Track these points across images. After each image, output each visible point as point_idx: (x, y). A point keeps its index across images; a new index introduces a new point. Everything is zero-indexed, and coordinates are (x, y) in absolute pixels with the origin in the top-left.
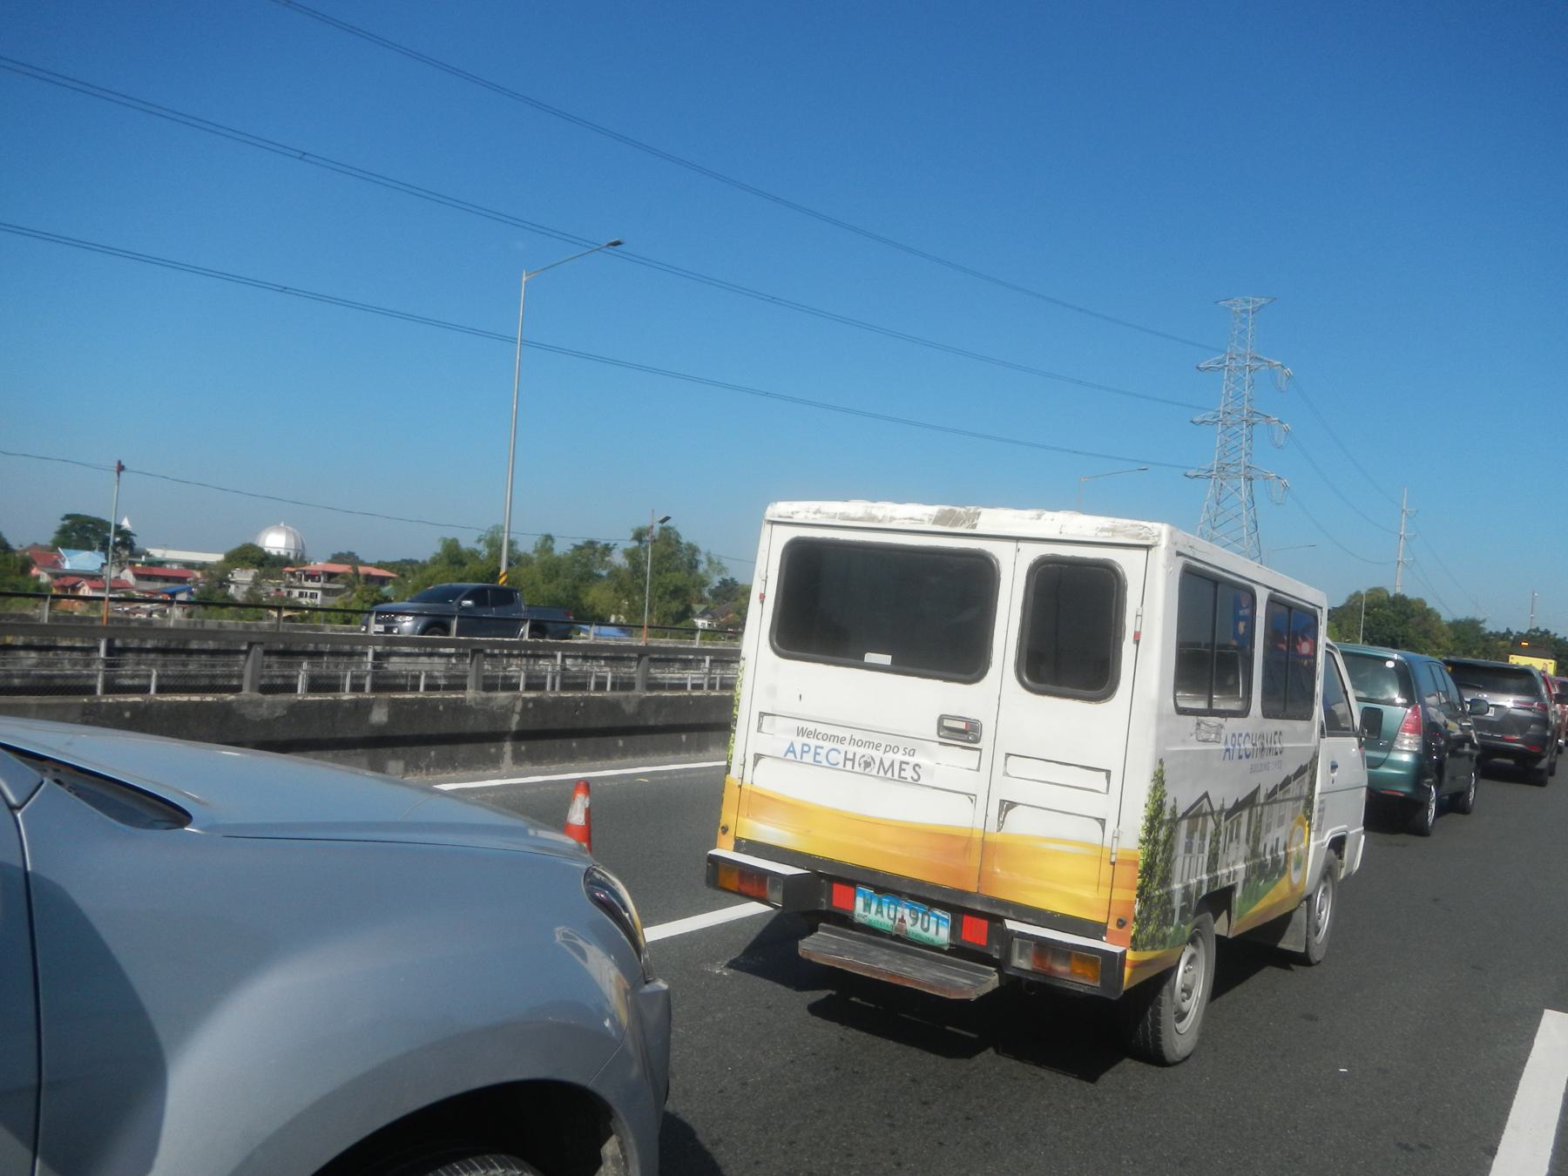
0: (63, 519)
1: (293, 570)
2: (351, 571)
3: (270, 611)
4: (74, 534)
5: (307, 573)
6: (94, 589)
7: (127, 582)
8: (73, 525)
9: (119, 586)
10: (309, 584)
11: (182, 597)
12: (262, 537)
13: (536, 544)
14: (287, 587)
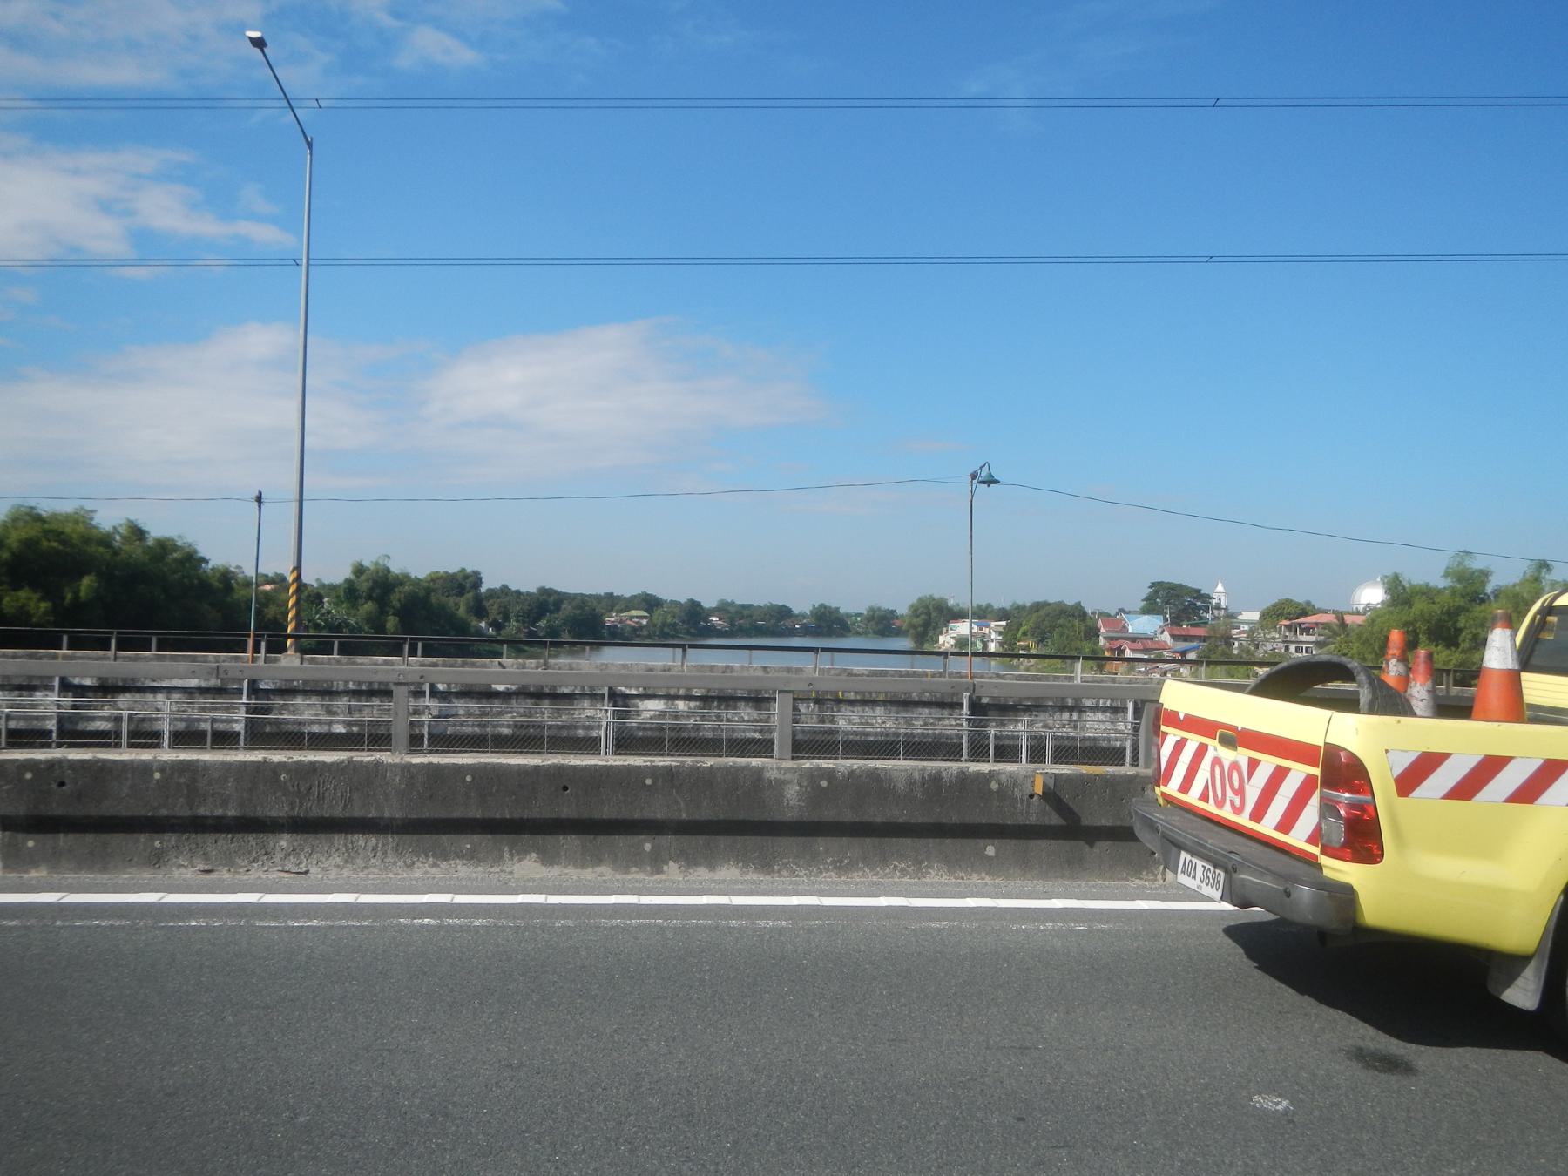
0: (1151, 587)
1: (1287, 623)
2: (1335, 621)
3: (1255, 668)
4: (1158, 600)
5: (1303, 626)
6: (1133, 650)
7: (1165, 642)
8: (1156, 592)
9: (1157, 646)
10: (1304, 638)
11: (1192, 656)
12: (1356, 597)
13: (1525, 573)
14: (1284, 642)
